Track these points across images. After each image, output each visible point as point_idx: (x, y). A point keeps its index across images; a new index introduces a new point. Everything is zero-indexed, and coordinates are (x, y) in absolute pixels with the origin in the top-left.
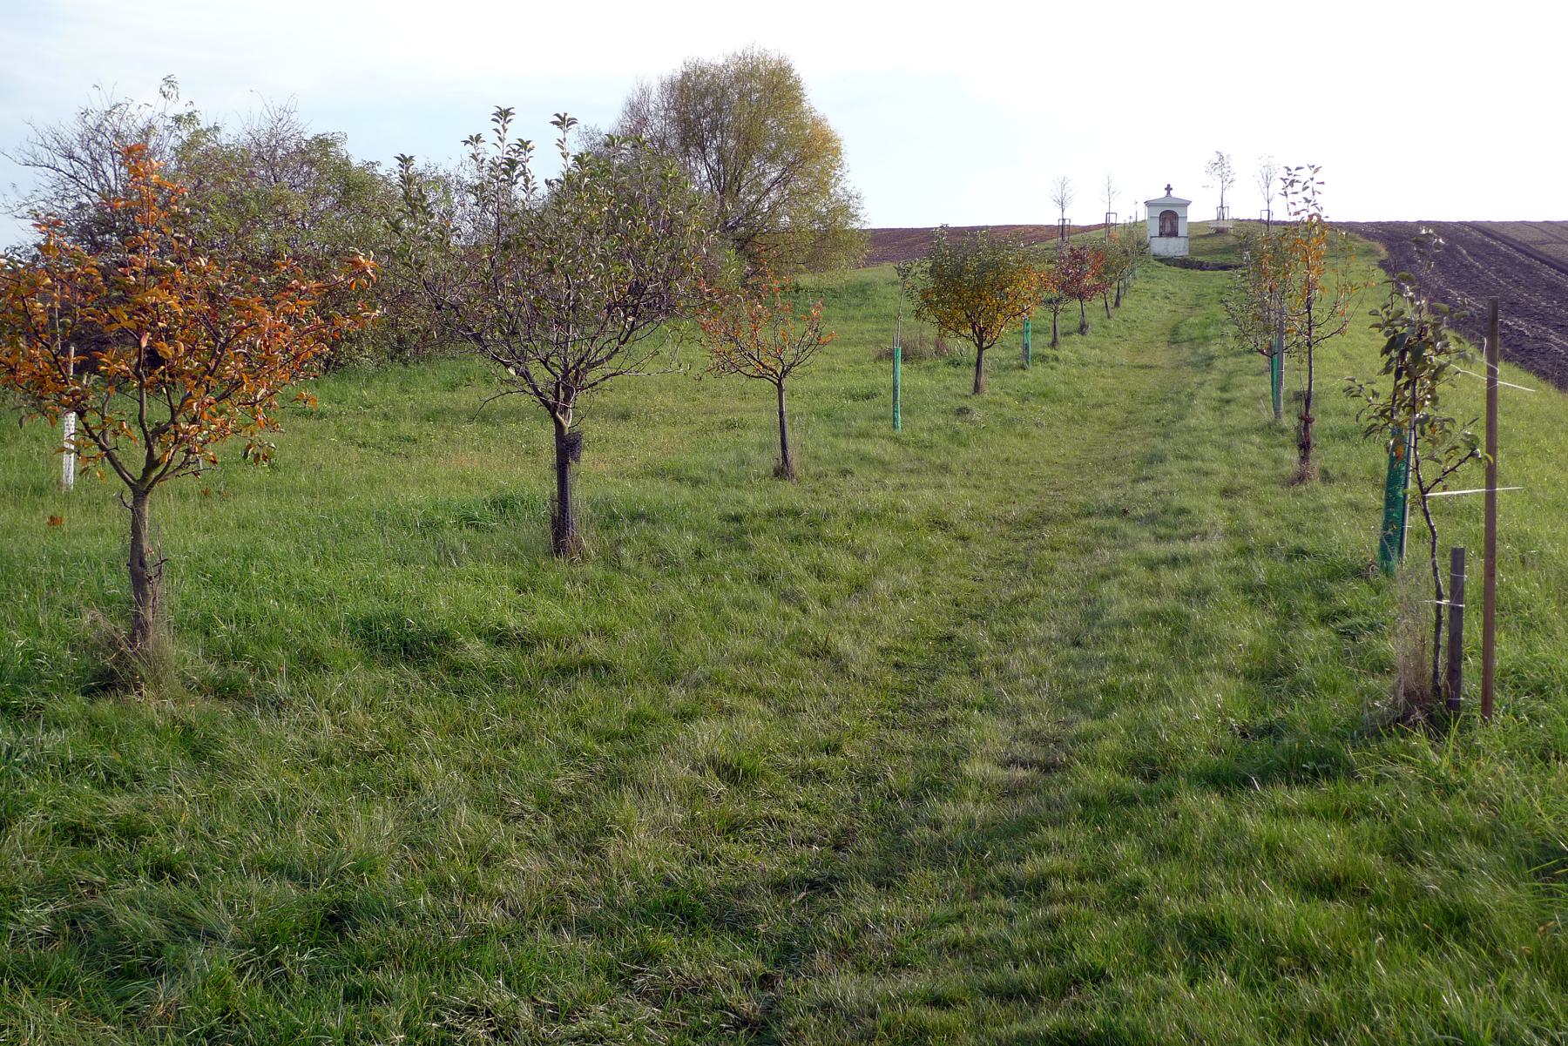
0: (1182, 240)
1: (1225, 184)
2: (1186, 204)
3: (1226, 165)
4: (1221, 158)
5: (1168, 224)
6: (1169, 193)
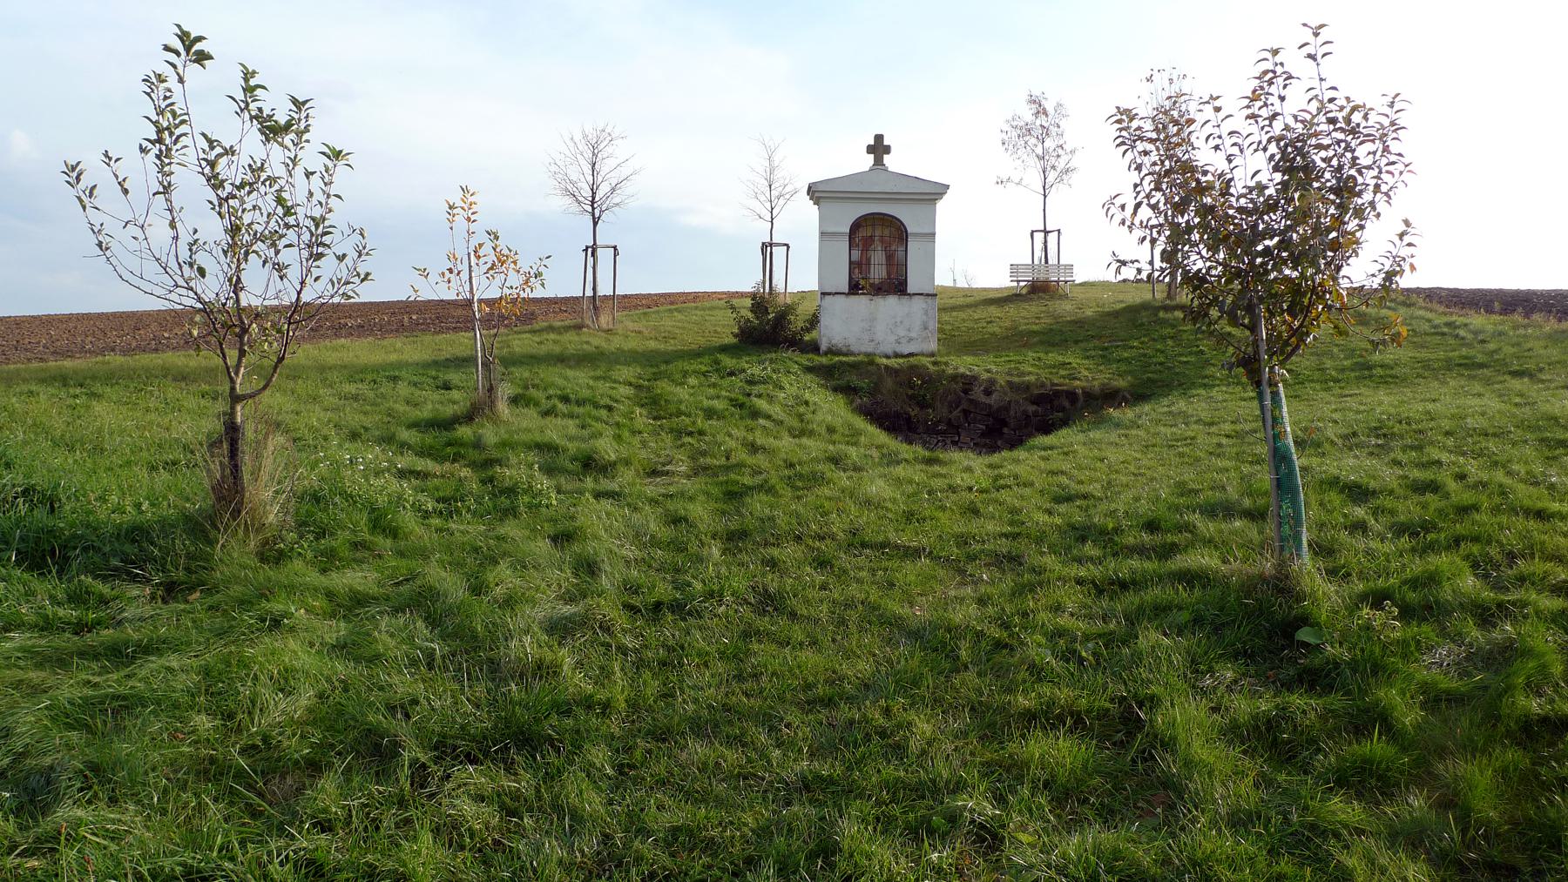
0: (918, 305)
1: (1052, 176)
2: (932, 194)
3: (1053, 130)
4: (1041, 111)
5: (878, 257)
6: (879, 162)
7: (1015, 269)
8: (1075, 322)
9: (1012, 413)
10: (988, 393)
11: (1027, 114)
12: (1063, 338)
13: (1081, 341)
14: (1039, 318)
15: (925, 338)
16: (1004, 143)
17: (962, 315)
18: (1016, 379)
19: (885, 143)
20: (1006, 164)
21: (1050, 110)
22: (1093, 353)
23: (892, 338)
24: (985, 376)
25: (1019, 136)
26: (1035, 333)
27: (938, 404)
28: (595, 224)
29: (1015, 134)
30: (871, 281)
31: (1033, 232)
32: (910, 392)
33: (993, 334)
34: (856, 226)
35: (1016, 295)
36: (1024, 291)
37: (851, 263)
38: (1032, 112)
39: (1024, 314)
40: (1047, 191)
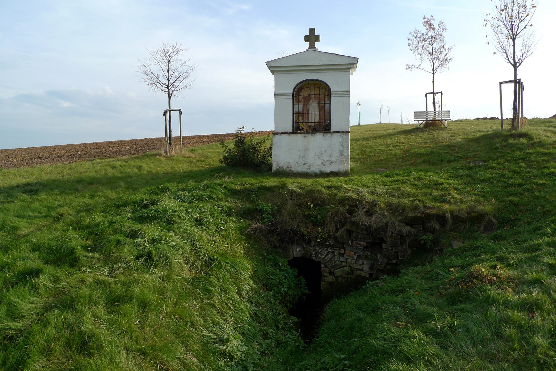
0: (336, 139)
1: (437, 64)
4: (430, 27)
5: (314, 109)
6: (312, 46)
7: (417, 114)
8: (448, 146)
9: (389, 233)
10: (369, 214)
11: (423, 30)
12: (439, 158)
13: (453, 161)
14: (426, 143)
15: (341, 162)
16: (409, 46)
17: (382, 141)
18: (395, 201)
20: (411, 57)
21: (436, 26)
22: (461, 172)
23: (319, 162)
24: (369, 198)
25: (418, 42)
26: (422, 154)
27: (327, 223)
28: (170, 98)
29: (416, 41)
30: (310, 124)
31: (426, 94)
32: (307, 212)
33: (395, 155)
35: (417, 128)
36: (422, 126)
38: (425, 28)
39: (419, 140)
40: (435, 72)
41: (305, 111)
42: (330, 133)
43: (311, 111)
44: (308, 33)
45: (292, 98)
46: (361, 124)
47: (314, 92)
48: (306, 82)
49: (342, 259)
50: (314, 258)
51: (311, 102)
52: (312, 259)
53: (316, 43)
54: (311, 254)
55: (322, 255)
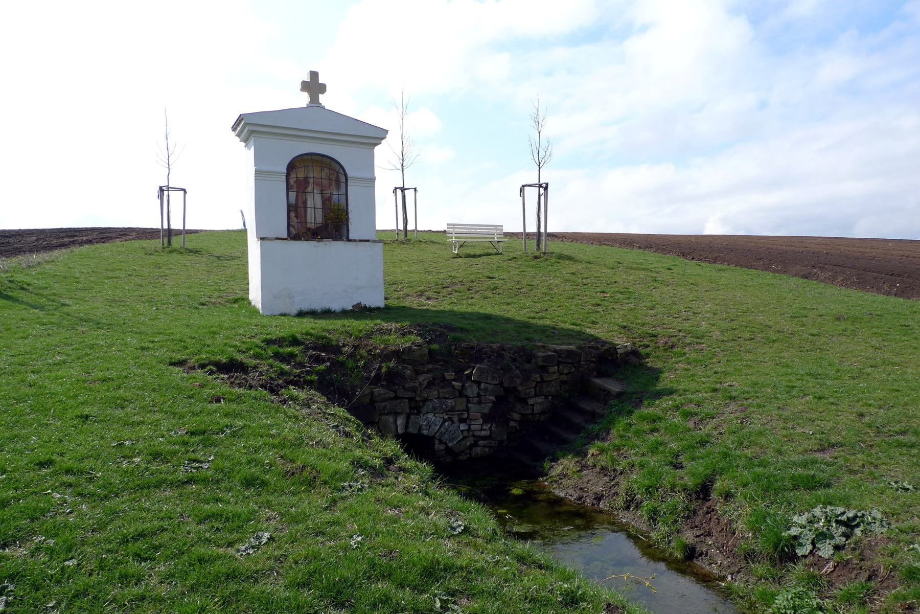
2: (375, 136)
5: (314, 201)
6: (314, 100)
19: (320, 81)
30: (308, 226)
34: (291, 166)
37: (289, 205)
41: (300, 204)
42: (348, 240)
43: (310, 204)
44: (307, 79)
45: (285, 180)
46: (418, 229)
47: (314, 174)
48: (309, 157)
49: (463, 427)
50: (425, 432)
51: (309, 189)
52: (423, 435)
53: (320, 95)
54: (420, 427)
55: (436, 425)
